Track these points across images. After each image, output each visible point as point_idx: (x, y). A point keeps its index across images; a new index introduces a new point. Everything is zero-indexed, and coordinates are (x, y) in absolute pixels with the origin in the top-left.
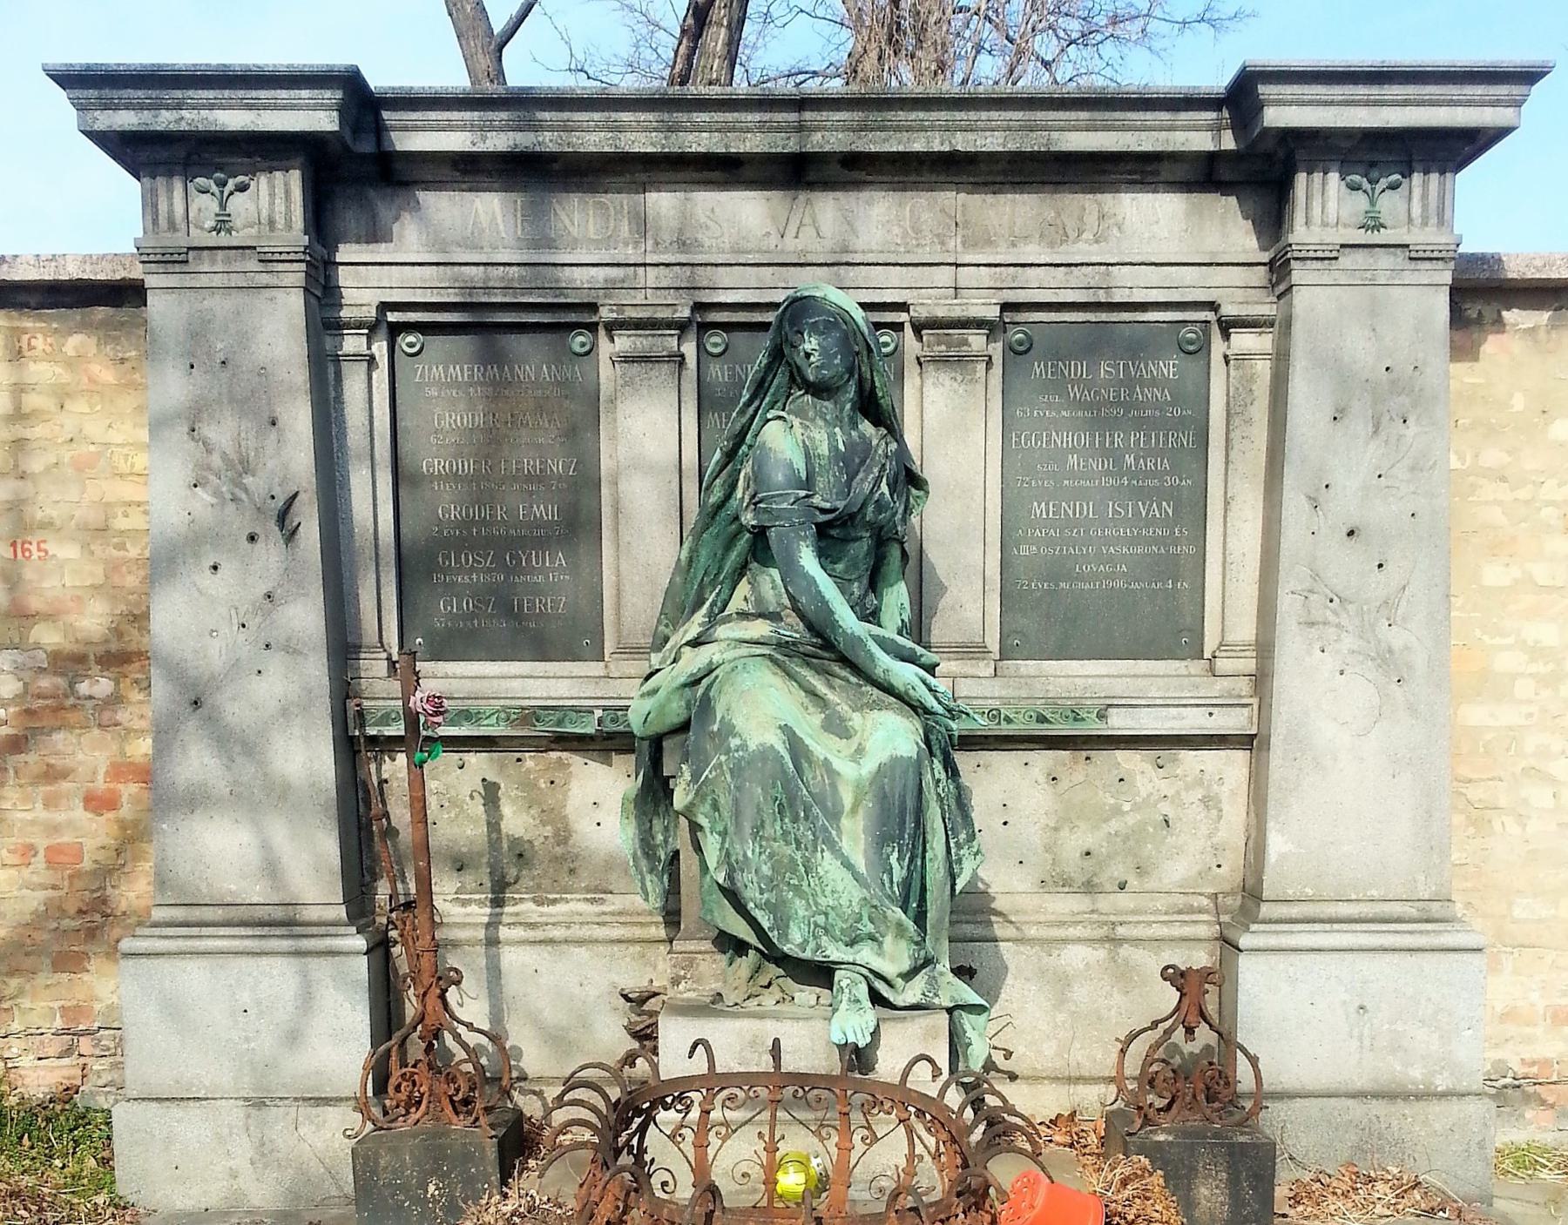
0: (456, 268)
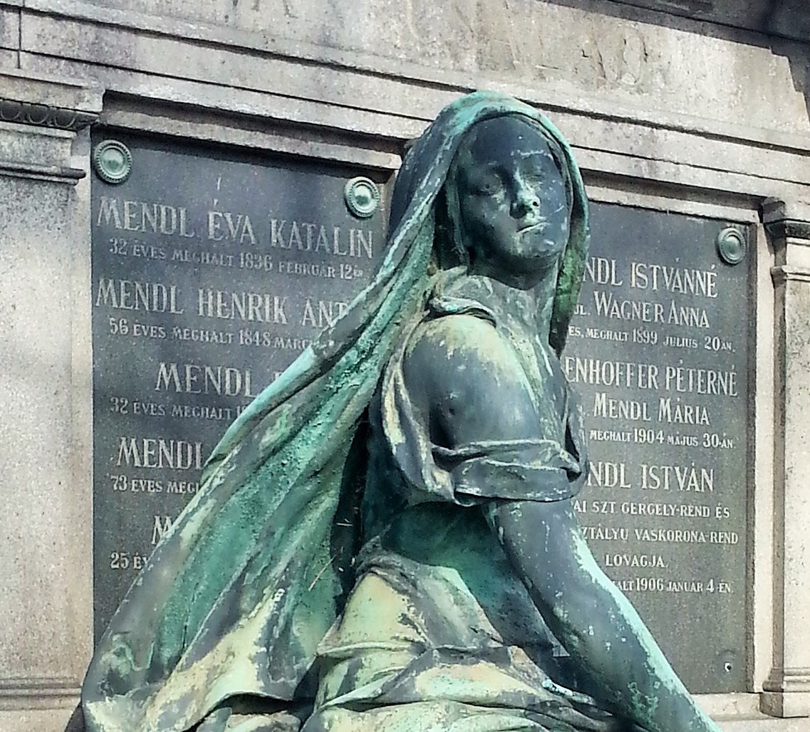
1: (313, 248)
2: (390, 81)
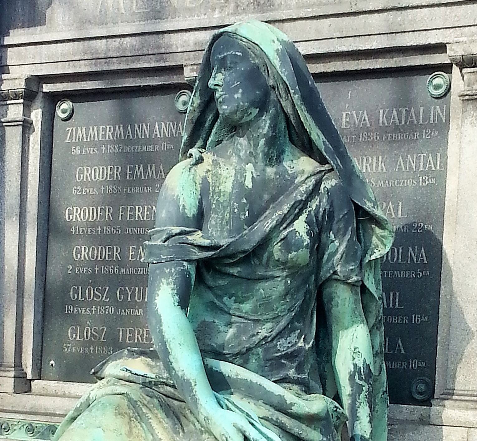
0: (86, 43)
1: (406, 123)
2: (436, 8)
